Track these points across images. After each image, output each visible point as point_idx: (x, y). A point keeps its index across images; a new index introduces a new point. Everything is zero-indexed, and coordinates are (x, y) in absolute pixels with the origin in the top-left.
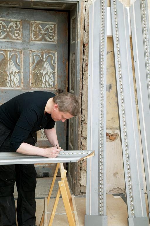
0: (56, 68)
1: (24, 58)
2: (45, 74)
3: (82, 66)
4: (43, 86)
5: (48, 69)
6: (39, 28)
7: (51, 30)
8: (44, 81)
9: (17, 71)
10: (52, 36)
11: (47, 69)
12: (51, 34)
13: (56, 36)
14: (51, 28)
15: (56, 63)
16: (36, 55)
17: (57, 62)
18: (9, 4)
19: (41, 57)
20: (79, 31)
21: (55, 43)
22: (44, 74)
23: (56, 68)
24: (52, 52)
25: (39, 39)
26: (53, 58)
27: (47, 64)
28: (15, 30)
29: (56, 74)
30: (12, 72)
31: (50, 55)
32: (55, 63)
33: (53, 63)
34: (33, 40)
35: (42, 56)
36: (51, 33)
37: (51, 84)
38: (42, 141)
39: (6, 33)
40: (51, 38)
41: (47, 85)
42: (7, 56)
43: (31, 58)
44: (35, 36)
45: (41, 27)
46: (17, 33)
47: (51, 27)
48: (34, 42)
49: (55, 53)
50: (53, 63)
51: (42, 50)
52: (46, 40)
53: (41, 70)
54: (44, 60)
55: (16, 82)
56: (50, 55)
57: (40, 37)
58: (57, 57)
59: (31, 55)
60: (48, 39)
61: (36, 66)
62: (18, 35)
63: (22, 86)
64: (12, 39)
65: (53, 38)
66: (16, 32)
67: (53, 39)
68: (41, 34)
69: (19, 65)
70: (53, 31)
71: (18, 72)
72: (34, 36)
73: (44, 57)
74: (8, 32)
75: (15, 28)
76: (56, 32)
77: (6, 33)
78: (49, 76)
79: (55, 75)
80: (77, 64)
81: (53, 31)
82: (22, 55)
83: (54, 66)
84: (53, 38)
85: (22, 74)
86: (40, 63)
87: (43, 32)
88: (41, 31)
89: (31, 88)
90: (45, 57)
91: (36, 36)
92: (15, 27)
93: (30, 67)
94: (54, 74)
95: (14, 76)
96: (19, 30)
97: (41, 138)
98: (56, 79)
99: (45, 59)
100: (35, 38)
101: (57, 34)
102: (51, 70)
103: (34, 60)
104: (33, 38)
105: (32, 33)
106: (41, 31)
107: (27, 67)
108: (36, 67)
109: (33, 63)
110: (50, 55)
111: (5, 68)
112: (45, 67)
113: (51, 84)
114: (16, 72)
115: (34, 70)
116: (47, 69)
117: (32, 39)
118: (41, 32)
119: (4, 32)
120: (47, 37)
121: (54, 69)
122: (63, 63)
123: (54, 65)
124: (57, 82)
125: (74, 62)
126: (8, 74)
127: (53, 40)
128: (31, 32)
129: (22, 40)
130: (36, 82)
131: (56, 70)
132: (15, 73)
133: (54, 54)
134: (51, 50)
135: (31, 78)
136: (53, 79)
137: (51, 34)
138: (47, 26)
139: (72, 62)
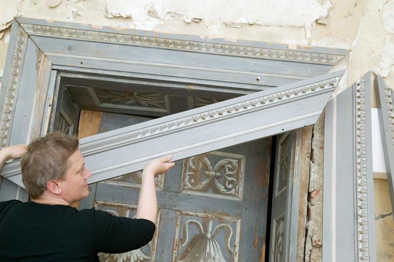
1: (162, 226)
3: (303, 246)
5: (217, 258)
6: (205, 165)
7: (230, 170)
10: (230, 182)
11: (214, 258)
12: (230, 179)
13: (240, 183)
14: (230, 166)
16: (191, 223)
17: (240, 243)
18: (140, 105)
19: (202, 228)
20: (296, 159)
21: (237, 199)
24: (228, 218)
25: (200, 186)
26: (230, 232)
27: (215, 246)
31: (224, 226)
32: (235, 246)
33: (229, 244)
34: (187, 189)
35: (205, 226)
36: (230, 176)
40: (230, 186)
44: (193, 181)
45: (209, 163)
47: (230, 163)
48: (189, 192)
49: (236, 222)
50: (229, 244)
51: (205, 212)
52: (217, 191)
54: (209, 236)
56: (224, 224)
57: (204, 183)
58: (241, 232)
59: (179, 220)
60: (222, 188)
61: (189, 249)
67: (234, 190)
68: (208, 176)
70: (235, 171)
72: (190, 179)
73: (210, 229)
76: (242, 175)
80: (290, 241)
81: (235, 171)
83: (230, 252)
87: (213, 173)
88: (208, 170)
90: (212, 230)
91: (195, 180)
93: (173, 249)
99: (211, 233)
100: (192, 184)
101: (243, 179)
103: (185, 233)
104: (188, 184)
105: (187, 174)
107: (166, 249)
108: (187, 252)
109: (182, 240)
110: (224, 224)
112: (209, 254)
114: (138, 259)
117: (185, 185)
118: (207, 172)
120: (219, 184)
122: (253, 247)
123: (232, 250)
125: (280, 239)
127: (233, 191)
128: (185, 171)
129: (162, 186)
133: (234, 225)
134: (227, 215)
137: (230, 179)
138: (222, 162)
139: (276, 241)
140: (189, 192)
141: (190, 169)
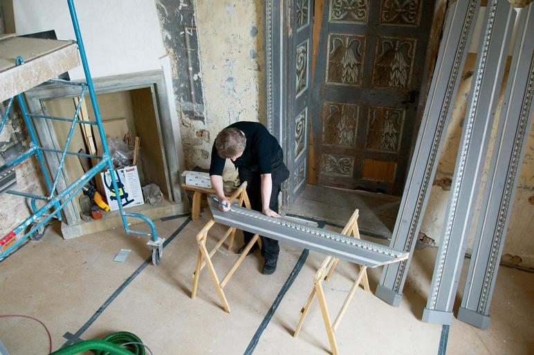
0: (413, 62)
2: (396, 69)
4: (390, 85)
7: (412, 7)
8: (392, 77)
9: (356, 62)
10: (412, 15)
12: (412, 13)
14: (412, 4)
15: (414, 54)
21: (415, 26)
22: (393, 68)
23: (413, 62)
24: (409, 39)
28: (360, 8)
29: (411, 70)
30: (349, 65)
35: (394, 43)
36: (412, 11)
37: (403, 82)
38: (380, 153)
39: (346, 13)
40: (412, 18)
41: (397, 83)
42: (345, 43)
43: (377, 47)
45: (398, 3)
46: (360, 12)
48: (384, 24)
52: (403, 22)
53: (390, 63)
54: (397, 49)
55: (353, 77)
57: (395, 17)
60: (406, 19)
62: (362, 14)
63: (361, 82)
64: (353, 21)
65: (415, 18)
66: (360, 10)
68: (397, 12)
69: (359, 55)
70: (416, 8)
71: (358, 65)
74: (349, 11)
75: (360, 6)
76: (420, 10)
77: (346, 13)
78: (401, 72)
79: (409, 71)
82: (365, 42)
84: (415, 18)
85: (362, 67)
86: (389, 54)
87: (400, 10)
88: (397, 8)
89: (373, 87)
92: (360, 3)
94: (408, 69)
95: (352, 69)
96: (364, 7)
97: (379, 149)
98: (410, 77)
100: (387, 19)
102: (405, 65)
106: (397, 8)
108: (383, 59)
109: (380, 52)
111: (341, 59)
112: (396, 60)
113: (403, 82)
115: (380, 62)
116: (399, 61)
117: (382, 19)
118: (396, 10)
119: (343, 11)
121: (409, 63)
124: (412, 82)
126: (345, 66)
127: (413, 21)
130: (380, 79)
131: (412, 65)
132: (353, 65)
133: (413, 42)
134: (408, 37)
135: (374, 73)
136: (405, 76)
137: (412, 13)
140: (384, 24)
141: (386, 9)
